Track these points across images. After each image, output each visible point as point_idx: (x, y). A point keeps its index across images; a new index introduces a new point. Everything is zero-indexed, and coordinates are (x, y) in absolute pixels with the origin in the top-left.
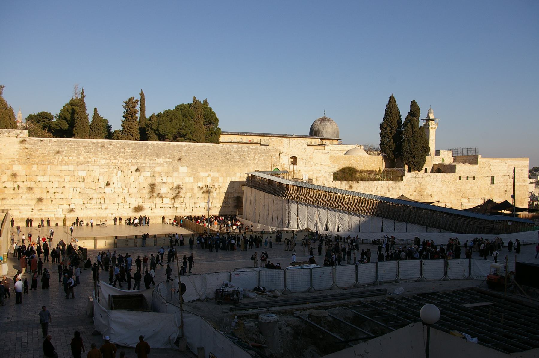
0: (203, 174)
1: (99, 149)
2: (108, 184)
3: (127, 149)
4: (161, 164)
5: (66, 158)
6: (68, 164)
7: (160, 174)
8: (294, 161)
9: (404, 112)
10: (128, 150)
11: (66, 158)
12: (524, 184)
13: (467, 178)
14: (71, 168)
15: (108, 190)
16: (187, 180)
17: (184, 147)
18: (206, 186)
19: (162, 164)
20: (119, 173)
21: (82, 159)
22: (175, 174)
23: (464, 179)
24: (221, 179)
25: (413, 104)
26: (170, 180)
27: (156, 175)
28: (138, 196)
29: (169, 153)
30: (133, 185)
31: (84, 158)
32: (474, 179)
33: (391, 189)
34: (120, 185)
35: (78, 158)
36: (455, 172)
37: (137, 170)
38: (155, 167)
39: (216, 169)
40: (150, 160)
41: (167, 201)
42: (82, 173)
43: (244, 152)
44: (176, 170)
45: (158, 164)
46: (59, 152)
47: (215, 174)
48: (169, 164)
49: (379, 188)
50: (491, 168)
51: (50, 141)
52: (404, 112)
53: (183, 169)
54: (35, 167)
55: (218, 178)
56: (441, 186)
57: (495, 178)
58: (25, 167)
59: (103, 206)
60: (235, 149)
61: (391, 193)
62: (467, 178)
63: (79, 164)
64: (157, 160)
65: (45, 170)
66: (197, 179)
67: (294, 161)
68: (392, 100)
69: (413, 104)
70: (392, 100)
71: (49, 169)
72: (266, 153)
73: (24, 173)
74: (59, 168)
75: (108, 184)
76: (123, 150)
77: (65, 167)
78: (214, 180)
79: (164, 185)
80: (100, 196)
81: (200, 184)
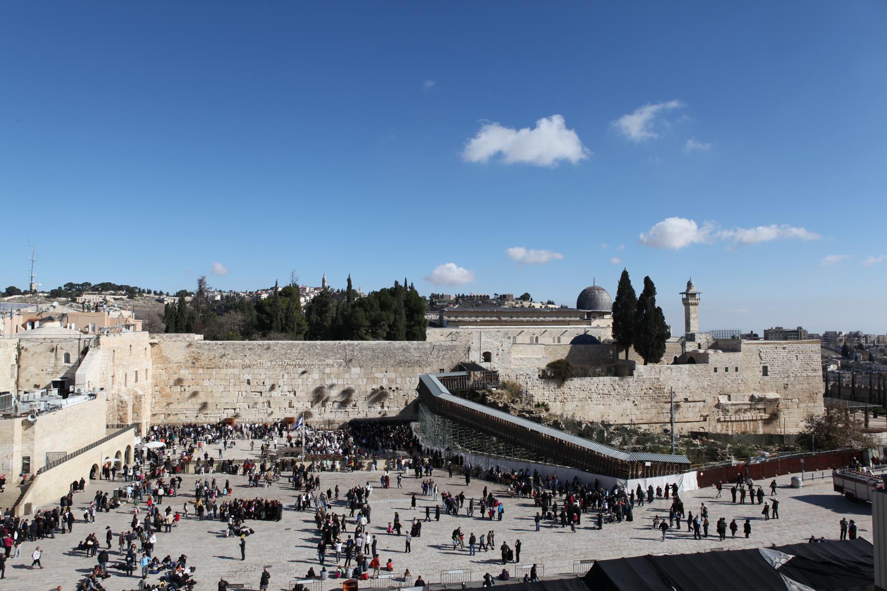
2: (273, 388)
6: (234, 367)
7: (329, 375)
8: (487, 357)
9: (639, 289)
12: (815, 374)
13: (727, 369)
14: (236, 371)
15: (273, 393)
18: (382, 388)
19: (333, 366)
20: (286, 376)
21: (247, 361)
22: (347, 376)
23: (721, 371)
24: (399, 380)
25: (647, 281)
26: (341, 382)
30: (300, 389)
32: (737, 370)
33: (617, 387)
34: (286, 389)
36: (707, 363)
37: (304, 373)
40: (320, 360)
42: (247, 377)
43: (425, 349)
47: (392, 375)
49: (601, 386)
50: (762, 354)
51: (216, 344)
52: (639, 289)
53: (356, 370)
56: (687, 380)
57: (769, 369)
58: (191, 371)
59: (269, 411)
60: (415, 346)
62: (727, 369)
63: (245, 367)
67: (487, 357)
68: (625, 275)
69: (647, 281)
70: (625, 275)
73: (190, 377)
74: (224, 371)
75: (273, 388)
77: (230, 371)
78: (390, 380)
80: (265, 400)
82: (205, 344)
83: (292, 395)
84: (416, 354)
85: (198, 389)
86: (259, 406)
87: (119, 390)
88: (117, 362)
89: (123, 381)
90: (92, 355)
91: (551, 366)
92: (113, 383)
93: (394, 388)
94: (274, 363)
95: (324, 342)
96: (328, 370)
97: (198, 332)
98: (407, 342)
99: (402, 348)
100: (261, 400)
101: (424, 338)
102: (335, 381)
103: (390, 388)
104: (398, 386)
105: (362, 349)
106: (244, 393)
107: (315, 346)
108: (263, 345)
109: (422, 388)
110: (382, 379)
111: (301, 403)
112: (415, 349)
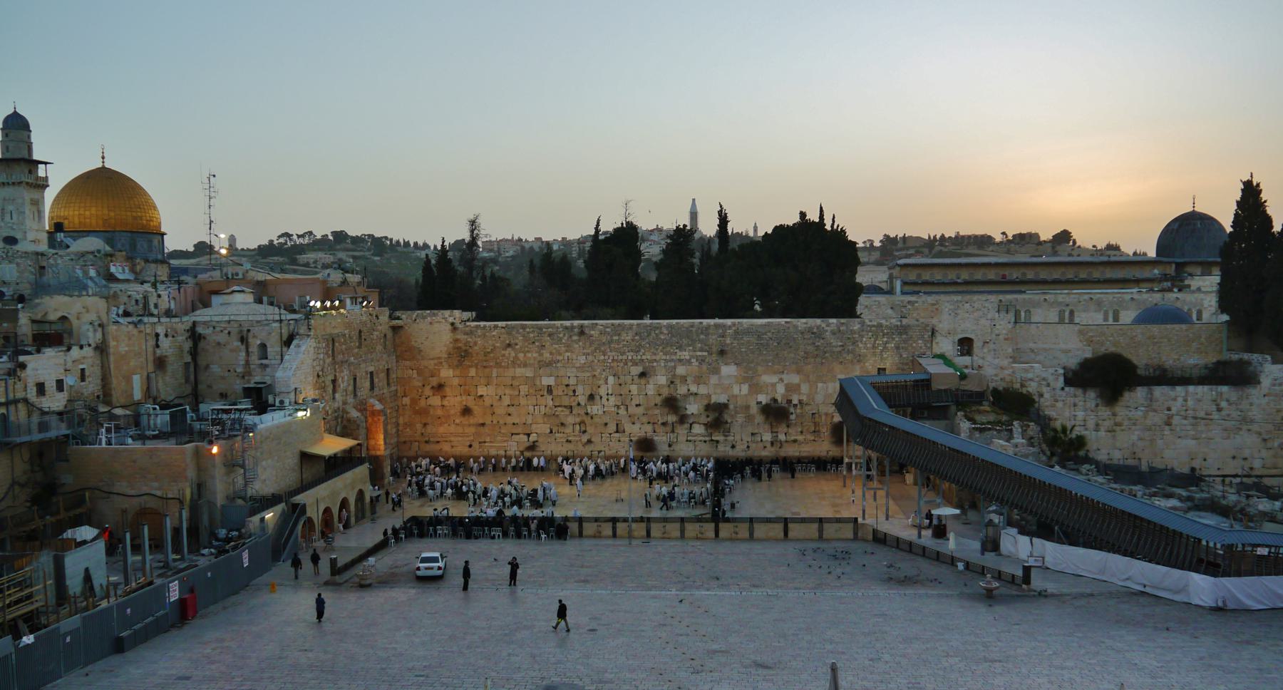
0: (768, 379)
1: (575, 338)
2: (591, 397)
3: (624, 335)
4: (687, 361)
5: (521, 355)
6: (525, 365)
7: (684, 379)
10: (627, 337)
11: (521, 355)
14: (529, 373)
16: (736, 390)
17: (730, 327)
18: (775, 400)
19: (689, 362)
20: (611, 380)
21: (547, 355)
22: (714, 380)
24: (805, 388)
26: (703, 390)
27: (677, 381)
28: (645, 419)
29: (701, 341)
31: (551, 353)
33: (1224, 404)
35: (541, 355)
37: (643, 375)
38: (675, 367)
39: (794, 367)
40: (665, 354)
41: (698, 429)
43: (853, 332)
44: (716, 371)
45: (680, 360)
46: (509, 345)
47: (795, 379)
48: (702, 361)
49: (1190, 403)
51: (496, 327)
53: (728, 370)
54: (472, 372)
55: (799, 385)
58: (458, 372)
59: (585, 438)
60: (833, 327)
61: (1223, 413)
64: (679, 353)
65: (489, 377)
66: (755, 388)
67: (966, 345)
71: (494, 374)
72: (900, 334)
73: (456, 381)
74: (510, 372)
76: (616, 338)
77: (519, 371)
78: (791, 388)
79: (692, 398)
80: (578, 420)
81: (764, 399)
82: (477, 327)
83: (622, 411)
84: (836, 342)
85: (470, 402)
86: (569, 430)
87: (345, 403)
88: (340, 357)
89: (351, 388)
90: (298, 346)
91: (1086, 365)
92: (334, 391)
93: (795, 402)
94: (590, 358)
95: (674, 322)
96: (681, 370)
97: (464, 309)
98: (818, 321)
99: (810, 330)
100: (570, 420)
101: (852, 314)
102: (693, 389)
103: (789, 402)
104: (804, 398)
105: (738, 334)
106: (543, 408)
107: (659, 327)
108: (573, 327)
109: (844, 401)
110: (775, 385)
111: (637, 426)
112: (833, 333)
